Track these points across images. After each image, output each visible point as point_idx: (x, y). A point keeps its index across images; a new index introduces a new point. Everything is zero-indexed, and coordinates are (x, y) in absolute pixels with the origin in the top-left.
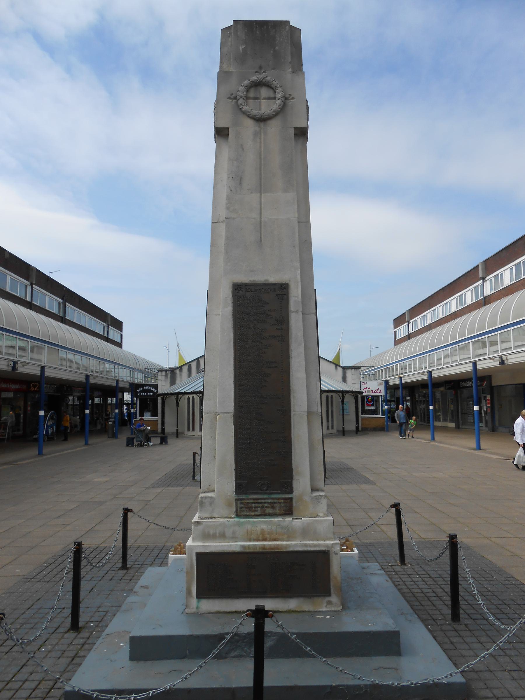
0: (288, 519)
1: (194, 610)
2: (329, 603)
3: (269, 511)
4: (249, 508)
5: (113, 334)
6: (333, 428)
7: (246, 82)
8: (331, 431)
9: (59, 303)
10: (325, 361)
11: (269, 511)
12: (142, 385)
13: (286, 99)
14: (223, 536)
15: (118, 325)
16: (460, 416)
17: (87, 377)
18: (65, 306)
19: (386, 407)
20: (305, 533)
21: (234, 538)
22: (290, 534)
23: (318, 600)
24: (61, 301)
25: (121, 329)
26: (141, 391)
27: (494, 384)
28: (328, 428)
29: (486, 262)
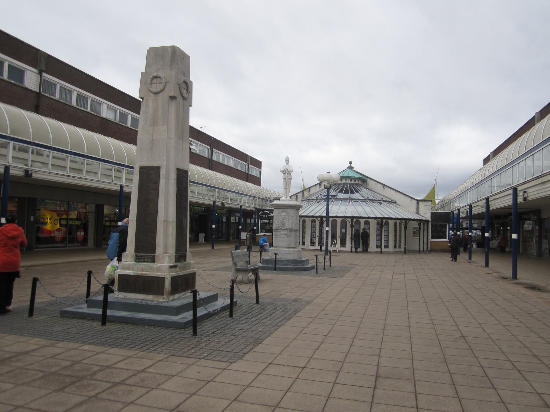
0: (152, 264)
1: (117, 296)
2: (164, 298)
3: (146, 260)
4: (139, 259)
5: (254, 171)
6: (400, 247)
7: (151, 77)
8: (397, 250)
9: (208, 149)
10: (398, 194)
11: (146, 260)
12: (263, 210)
13: (166, 83)
14: (128, 269)
15: (258, 164)
16: (521, 244)
17: (223, 204)
18: (212, 150)
19: (452, 233)
20: (158, 269)
21: (133, 270)
22: (152, 269)
23: (160, 296)
24: (209, 147)
25: (260, 167)
26: (262, 214)
27: (542, 217)
28: (395, 247)
29: (541, 111)
